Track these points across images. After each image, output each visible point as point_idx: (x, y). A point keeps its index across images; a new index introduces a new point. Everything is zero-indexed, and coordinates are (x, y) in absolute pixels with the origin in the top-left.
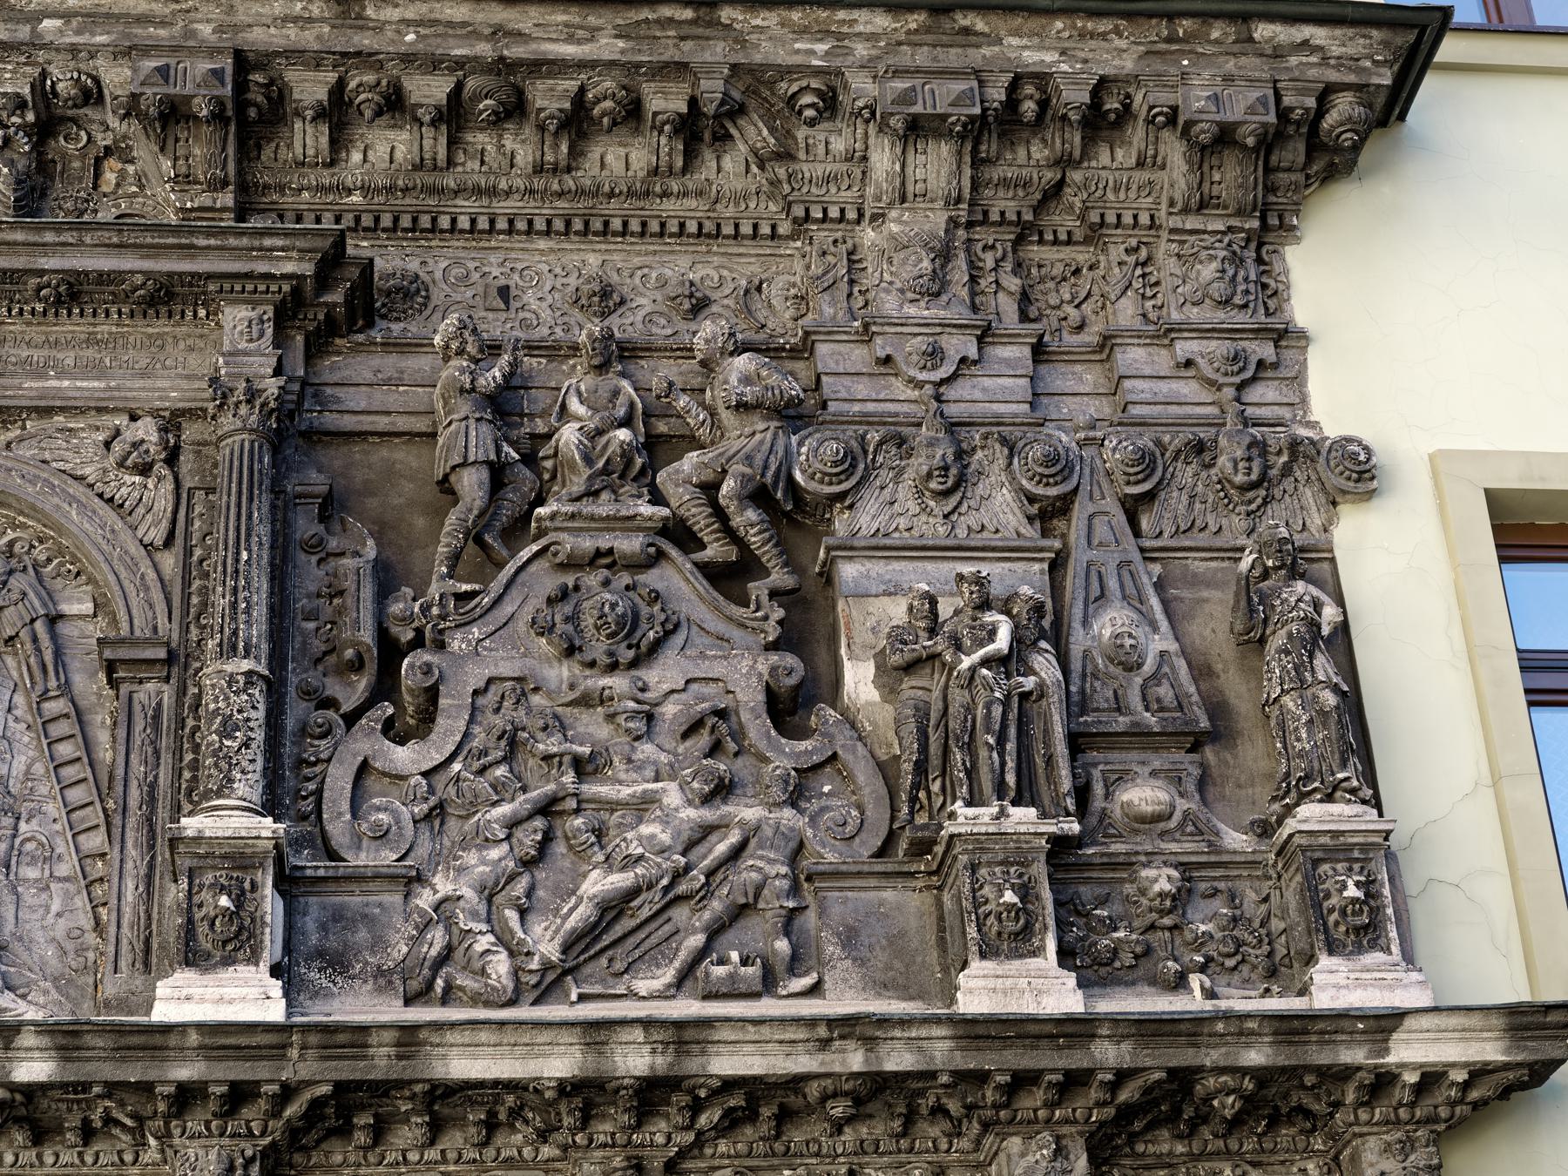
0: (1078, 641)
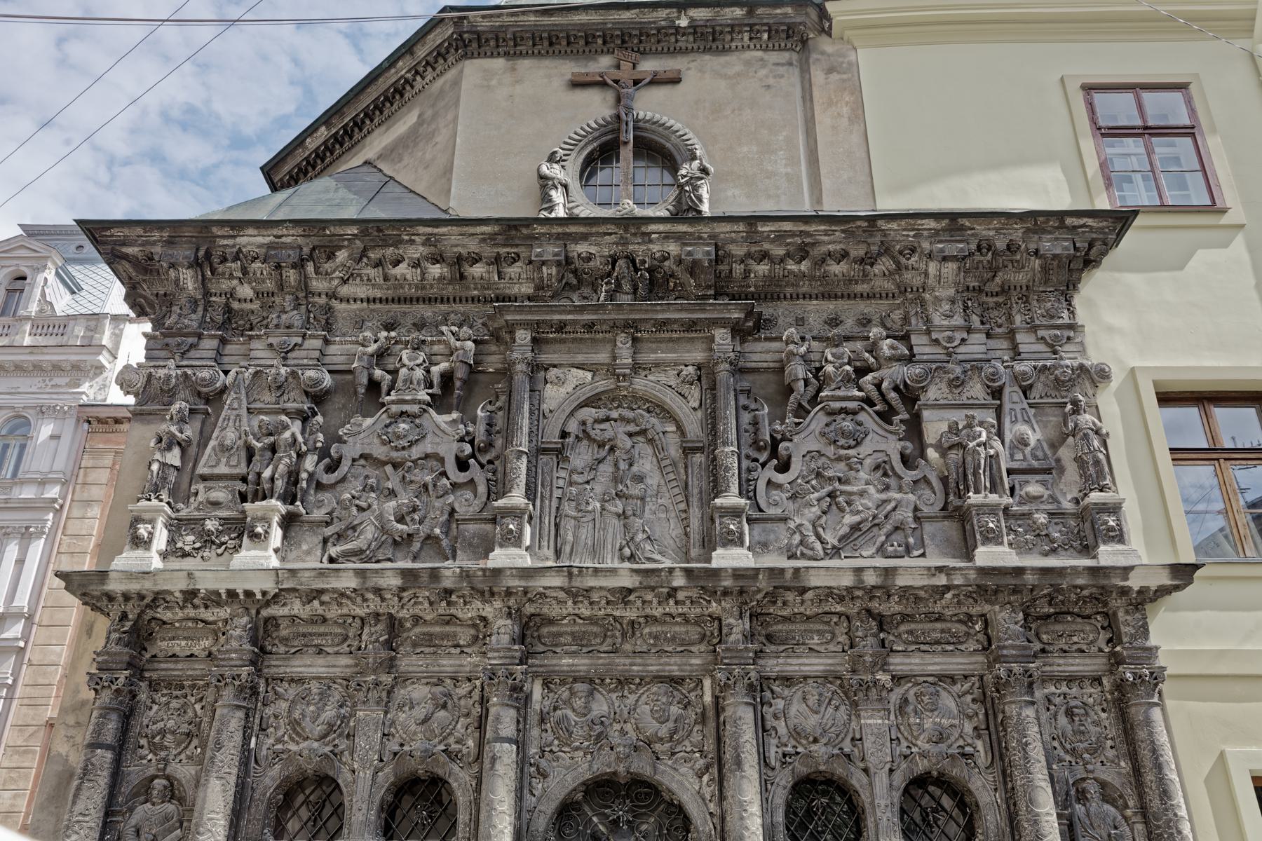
0: (1008, 436)
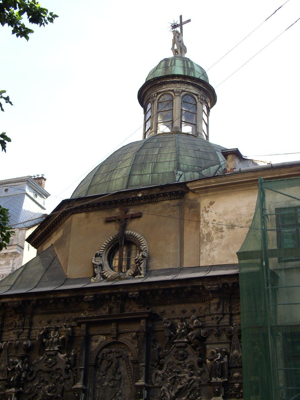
0: (231, 354)
